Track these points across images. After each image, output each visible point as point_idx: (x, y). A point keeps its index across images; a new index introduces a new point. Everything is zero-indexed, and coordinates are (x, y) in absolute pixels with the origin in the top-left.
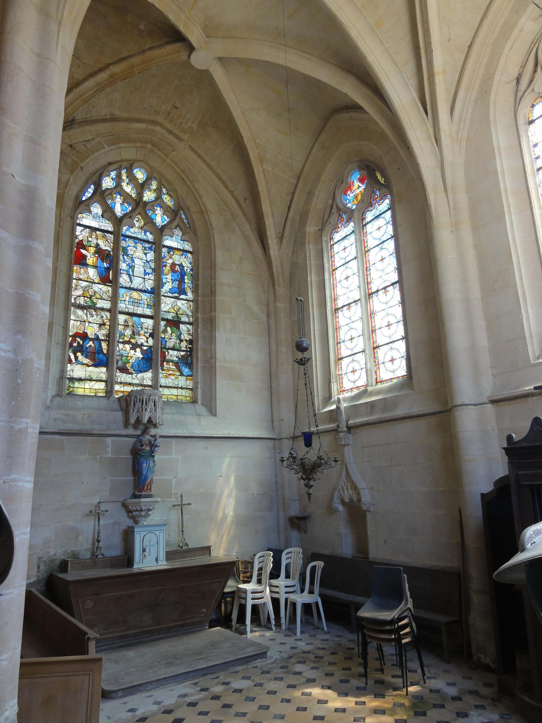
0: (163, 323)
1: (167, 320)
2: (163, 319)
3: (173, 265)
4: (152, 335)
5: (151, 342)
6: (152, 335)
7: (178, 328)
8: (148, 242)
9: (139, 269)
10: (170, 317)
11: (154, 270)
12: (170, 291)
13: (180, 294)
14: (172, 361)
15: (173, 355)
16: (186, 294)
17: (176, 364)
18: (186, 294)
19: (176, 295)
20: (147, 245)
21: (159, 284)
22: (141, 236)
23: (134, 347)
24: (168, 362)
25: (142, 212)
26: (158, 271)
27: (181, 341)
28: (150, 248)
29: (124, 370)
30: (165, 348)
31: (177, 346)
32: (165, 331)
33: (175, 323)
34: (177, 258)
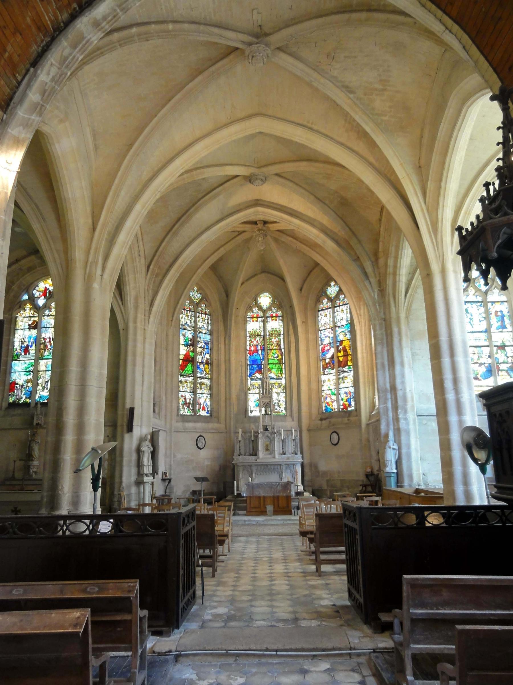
0: (495, 348)
1: (497, 346)
2: (495, 346)
3: (496, 312)
4: (489, 357)
5: (490, 361)
6: (489, 357)
7: (505, 350)
8: (479, 302)
9: (476, 321)
10: (499, 344)
11: (485, 318)
12: (498, 329)
13: (503, 329)
14: (504, 370)
15: (503, 367)
16: (506, 328)
17: (507, 371)
18: (506, 328)
19: (501, 330)
20: (479, 304)
21: (489, 325)
22: (474, 299)
23: (481, 364)
24: (502, 370)
25: (473, 285)
26: (487, 318)
27: (508, 357)
28: (481, 306)
29: (476, 378)
30: (498, 363)
31: (506, 361)
32: (497, 353)
33: (502, 347)
34: (498, 307)
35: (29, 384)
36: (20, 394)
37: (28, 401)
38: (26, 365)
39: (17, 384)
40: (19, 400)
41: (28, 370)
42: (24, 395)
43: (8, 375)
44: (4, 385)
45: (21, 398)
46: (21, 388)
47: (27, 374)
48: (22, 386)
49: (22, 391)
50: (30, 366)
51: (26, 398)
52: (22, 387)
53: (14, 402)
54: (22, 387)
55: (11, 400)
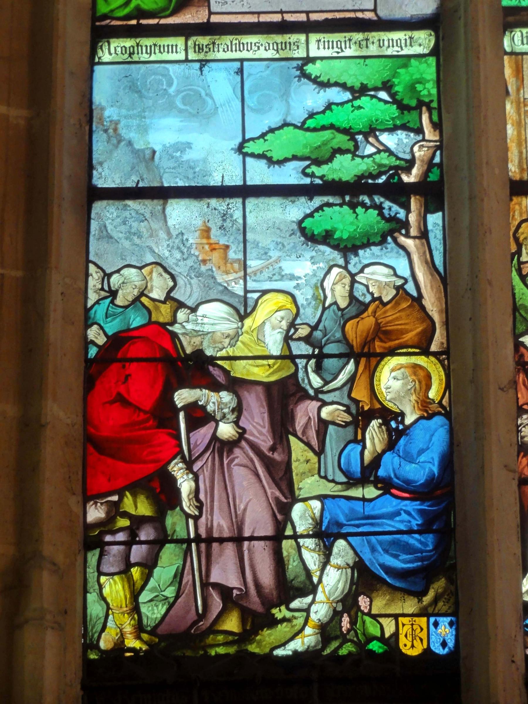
35: (392, 379)
36: (258, 519)
37: (419, 632)
38: (312, 99)
39: (199, 368)
40: (259, 620)
41: (345, 168)
42: (325, 535)
43: (64, 219)
44: (29, 388)
45: (291, 587)
46: (258, 425)
47: (342, 219)
48: (284, 396)
49: (281, 475)
50: (375, 108)
51: (364, 580)
52: (282, 425)
53: (174, 647)
54: (282, 425)
55: (117, 608)
